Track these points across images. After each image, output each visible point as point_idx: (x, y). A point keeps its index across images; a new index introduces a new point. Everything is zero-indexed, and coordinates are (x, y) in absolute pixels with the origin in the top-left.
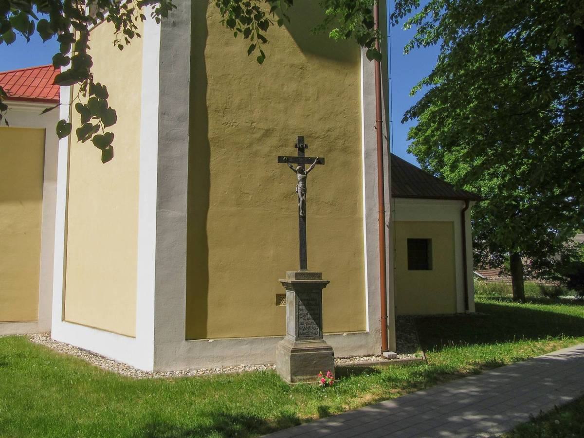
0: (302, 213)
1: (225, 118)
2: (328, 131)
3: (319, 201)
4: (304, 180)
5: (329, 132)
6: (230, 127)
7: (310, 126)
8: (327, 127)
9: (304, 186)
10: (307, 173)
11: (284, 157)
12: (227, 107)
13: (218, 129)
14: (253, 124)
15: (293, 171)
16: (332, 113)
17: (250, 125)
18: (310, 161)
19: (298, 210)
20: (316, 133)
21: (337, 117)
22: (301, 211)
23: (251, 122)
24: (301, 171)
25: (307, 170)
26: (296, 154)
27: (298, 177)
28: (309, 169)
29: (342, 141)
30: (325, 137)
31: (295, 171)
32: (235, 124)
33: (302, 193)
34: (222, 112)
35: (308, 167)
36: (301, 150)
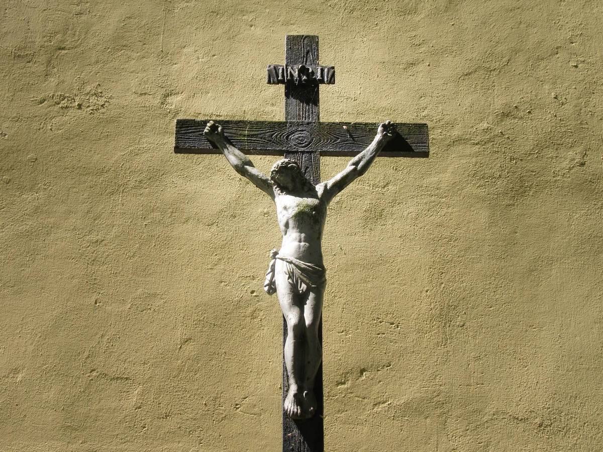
0: (298, 399)
1: (53, 81)
2: (505, 115)
3: (478, 411)
4: (310, 223)
5: (508, 122)
6: (71, 112)
7: (423, 102)
8: (498, 103)
9: (312, 251)
10: (330, 193)
11: (205, 123)
12: (67, 44)
13: (17, 119)
14: (169, 100)
15: (252, 187)
16: (516, 51)
17: (157, 102)
18: (348, 138)
19: (280, 382)
20: (452, 125)
21: (543, 64)
22: (293, 389)
23: (163, 91)
24: (294, 181)
25: (330, 183)
26: (273, 105)
27: (279, 208)
28: (338, 177)
29: (573, 154)
30: (489, 141)
31: (262, 184)
32: (93, 100)
33: (294, 288)
34: (43, 58)
35: (334, 169)
36: (304, 88)
